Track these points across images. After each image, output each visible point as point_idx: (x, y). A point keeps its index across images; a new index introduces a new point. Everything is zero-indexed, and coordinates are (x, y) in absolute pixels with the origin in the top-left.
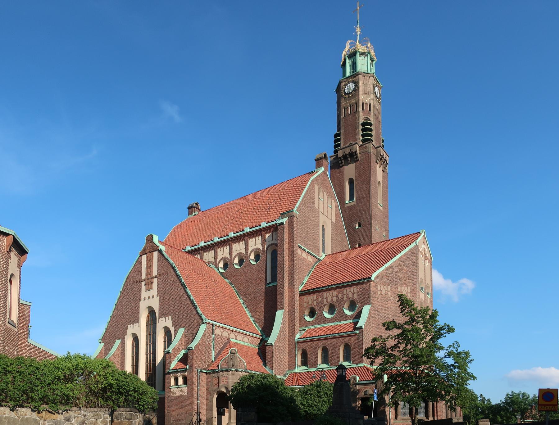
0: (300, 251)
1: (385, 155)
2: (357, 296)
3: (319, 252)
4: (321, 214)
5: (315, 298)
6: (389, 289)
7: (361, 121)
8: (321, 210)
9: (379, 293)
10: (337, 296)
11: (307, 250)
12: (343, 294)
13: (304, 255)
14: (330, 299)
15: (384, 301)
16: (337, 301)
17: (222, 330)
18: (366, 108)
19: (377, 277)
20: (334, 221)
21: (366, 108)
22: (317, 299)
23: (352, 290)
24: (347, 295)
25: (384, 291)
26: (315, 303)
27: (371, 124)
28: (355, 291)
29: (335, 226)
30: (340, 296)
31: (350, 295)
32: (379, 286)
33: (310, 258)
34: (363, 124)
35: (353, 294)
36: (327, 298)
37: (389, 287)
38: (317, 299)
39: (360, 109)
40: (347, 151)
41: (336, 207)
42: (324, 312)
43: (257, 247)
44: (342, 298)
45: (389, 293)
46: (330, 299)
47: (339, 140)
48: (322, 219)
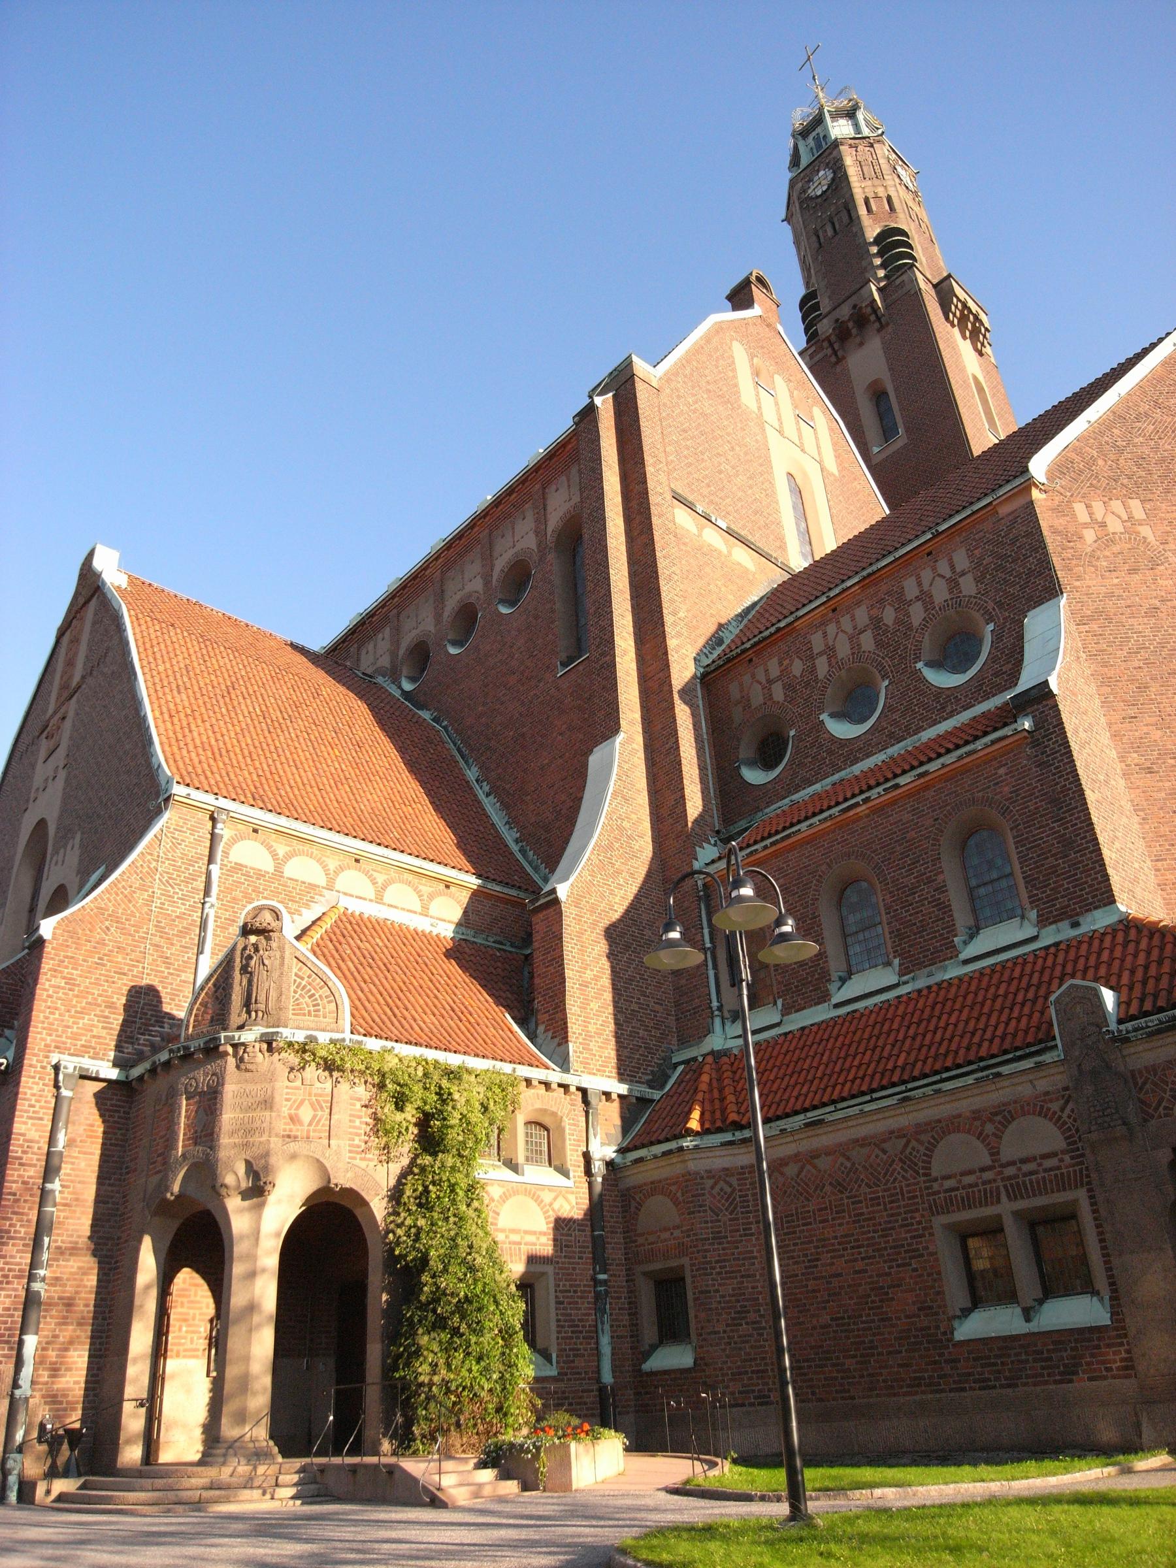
0: (682, 516)
1: (971, 304)
2: (978, 580)
3: (783, 547)
4: (772, 435)
5: (775, 671)
6: (1138, 511)
7: (872, 231)
8: (769, 415)
9: (1089, 535)
10: (876, 623)
11: (721, 523)
12: (902, 604)
13: (713, 538)
14: (843, 649)
15: (1133, 571)
16: (879, 644)
17: (282, 850)
18: (881, 206)
19: (1059, 468)
20: (832, 465)
21: (881, 206)
22: (785, 672)
23: (943, 567)
24: (925, 597)
25: (1115, 526)
26: (778, 693)
27: (903, 233)
28: (961, 560)
29: (835, 486)
30: (889, 616)
31: (940, 593)
32: (1079, 508)
33: (742, 556)
34: (878, 240)
35: (953, 584)
36: (830, 651)
37: (1135, 504)
38: (785, 672)
39: (862, 211)
40: (845, 311)
41: (831, 430)
42: (824, 717)
43: (519, 547)
44: (903, 622)
45: (1146, 531)
46: (843, 649)
47: (816, 307)
48: (782, 457)
